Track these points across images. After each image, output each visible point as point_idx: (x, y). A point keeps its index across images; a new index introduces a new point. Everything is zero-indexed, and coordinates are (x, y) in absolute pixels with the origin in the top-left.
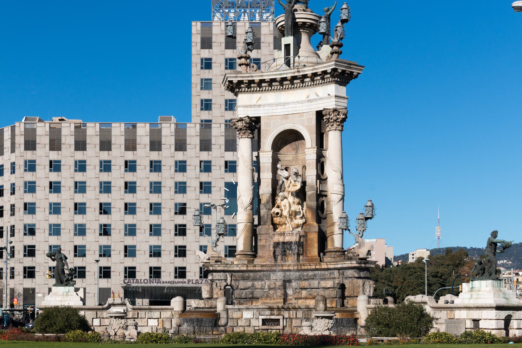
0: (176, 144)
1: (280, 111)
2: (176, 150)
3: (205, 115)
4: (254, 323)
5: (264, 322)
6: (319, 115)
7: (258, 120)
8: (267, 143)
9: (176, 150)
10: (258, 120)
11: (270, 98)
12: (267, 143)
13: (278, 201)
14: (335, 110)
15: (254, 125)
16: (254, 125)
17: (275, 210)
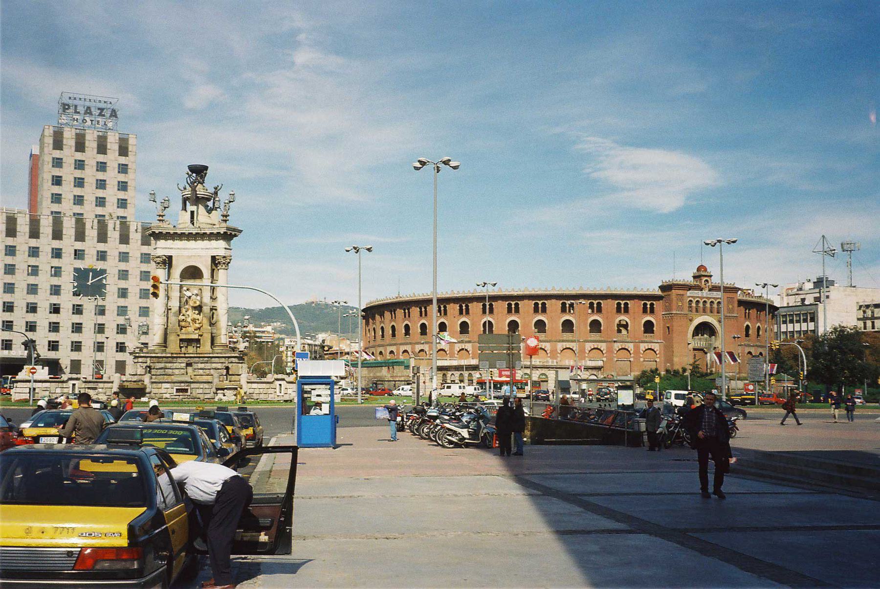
0: (30, 232)
1: (186, 253)
2: (30, 237)
3: (55, 207)
4: (170, 391)
5: (178, 390)
6: (213, 258)
7: (170, 258)
8: (177, 272)
9: (30, 237)
10: (170, 258)
11: (178, 244)
12: (177, 272)
13: (183, 311)
14: (224, 257)
15: (168, 262)
16: (168, 262)
17: (181, 317)
